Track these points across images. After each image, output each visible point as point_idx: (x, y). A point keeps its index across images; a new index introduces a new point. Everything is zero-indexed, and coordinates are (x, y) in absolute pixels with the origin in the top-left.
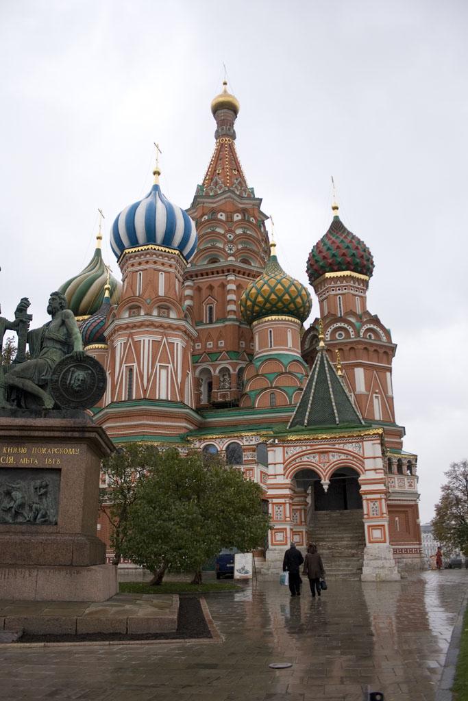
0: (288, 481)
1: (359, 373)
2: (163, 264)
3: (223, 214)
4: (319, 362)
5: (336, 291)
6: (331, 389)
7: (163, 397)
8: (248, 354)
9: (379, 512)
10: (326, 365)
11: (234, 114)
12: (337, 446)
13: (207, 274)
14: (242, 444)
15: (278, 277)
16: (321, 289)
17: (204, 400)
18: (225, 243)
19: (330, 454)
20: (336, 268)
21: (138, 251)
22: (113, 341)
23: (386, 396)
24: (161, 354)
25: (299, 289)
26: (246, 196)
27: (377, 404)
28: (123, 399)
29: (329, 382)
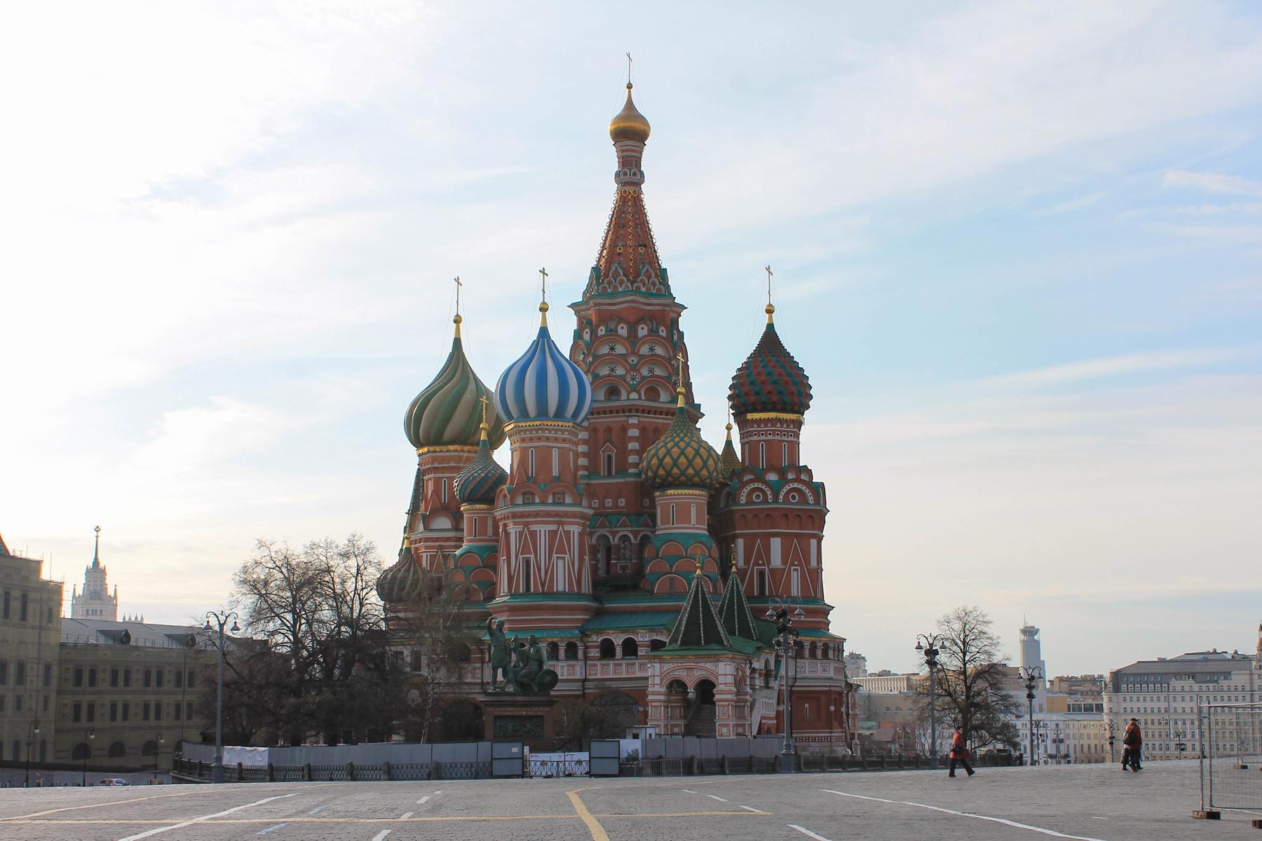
0: (663, 690)
1: (776, 543)
2: (556, 440)
3: (625, 326)
7: (561, 588)
9: (727, 715)
11: (641, 145)
13: (605, 413)
15: (682, 445)
17: (601, 573)
18: (627, 371)
20: (759, 407)
21: (529, 426)
24: (557, 544)
25: (705, 458)
26: (654, 292)
27: (795, 577)
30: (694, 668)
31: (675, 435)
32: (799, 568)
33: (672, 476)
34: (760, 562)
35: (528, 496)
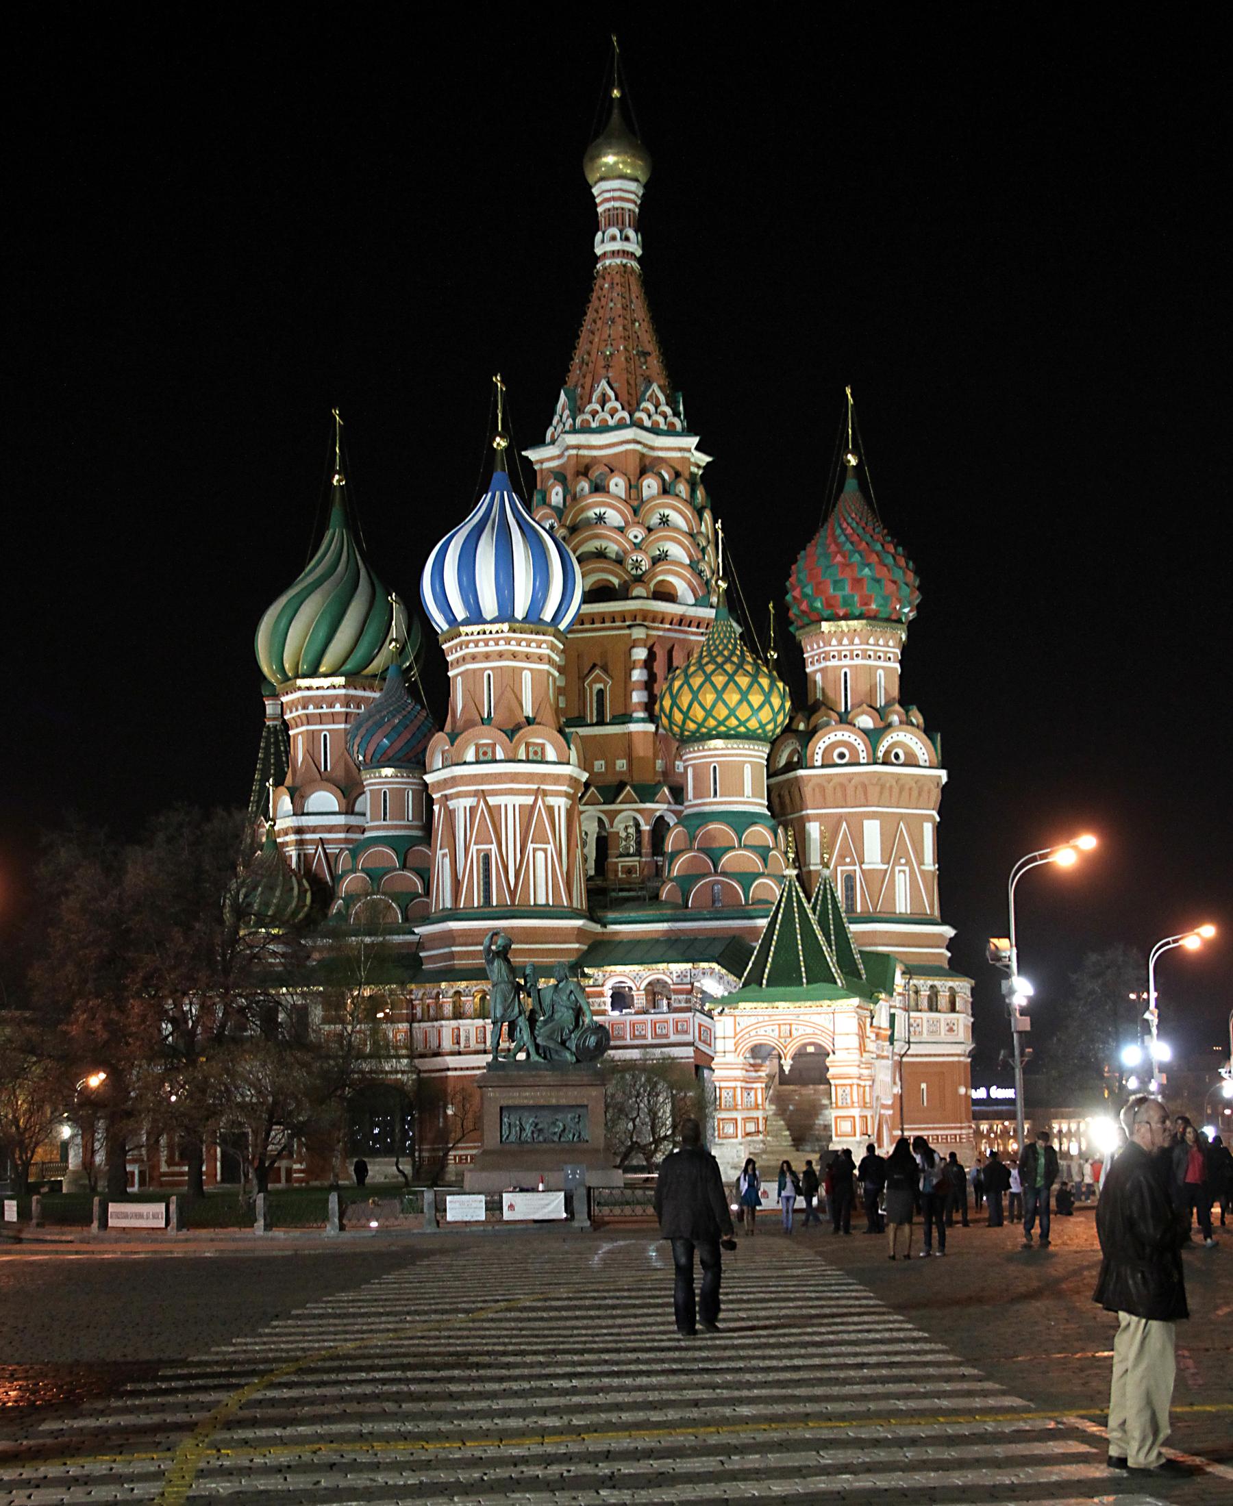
0: (741, 1059)
1: (872, 829)
2: (528, 657)
4: (785, 894)
5: (840, 659)
6: (799, 937)
7: (541, 900)
8: (671, 789)
9: (849, 1101)
10: (795, 899)
12: (802, 1017)
14: (670, 981)
16: (813, 650)
19: (794, 1027)
22: (446, 798)
23: (919, 868)
28: (476, 905)
29: (797, 926)
30: (790, 1025)
31: (715, 653)
32: (907, 869)
33: (714, 718)
34: (848, 860)
35: (485, 749)
